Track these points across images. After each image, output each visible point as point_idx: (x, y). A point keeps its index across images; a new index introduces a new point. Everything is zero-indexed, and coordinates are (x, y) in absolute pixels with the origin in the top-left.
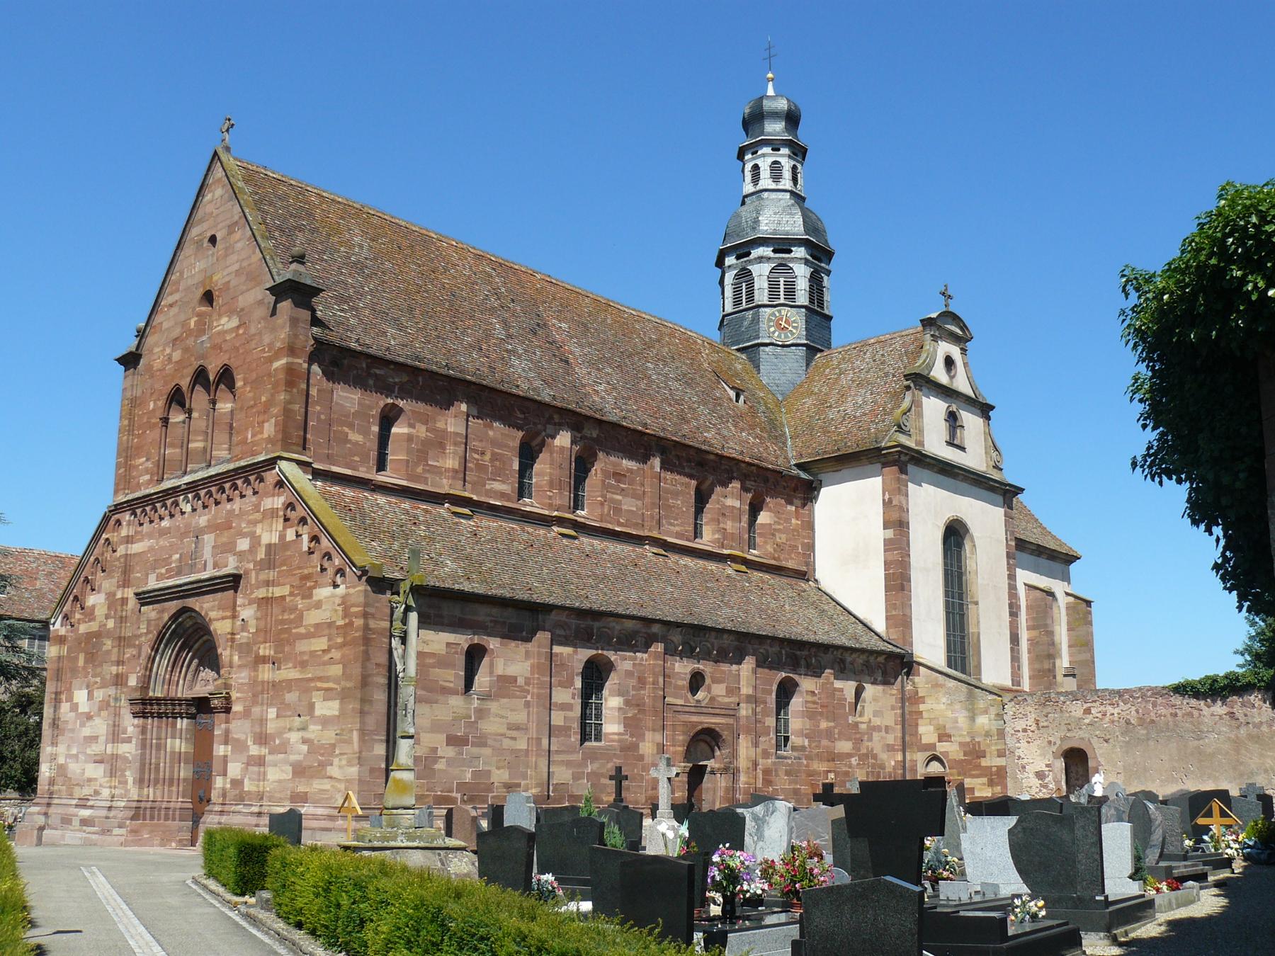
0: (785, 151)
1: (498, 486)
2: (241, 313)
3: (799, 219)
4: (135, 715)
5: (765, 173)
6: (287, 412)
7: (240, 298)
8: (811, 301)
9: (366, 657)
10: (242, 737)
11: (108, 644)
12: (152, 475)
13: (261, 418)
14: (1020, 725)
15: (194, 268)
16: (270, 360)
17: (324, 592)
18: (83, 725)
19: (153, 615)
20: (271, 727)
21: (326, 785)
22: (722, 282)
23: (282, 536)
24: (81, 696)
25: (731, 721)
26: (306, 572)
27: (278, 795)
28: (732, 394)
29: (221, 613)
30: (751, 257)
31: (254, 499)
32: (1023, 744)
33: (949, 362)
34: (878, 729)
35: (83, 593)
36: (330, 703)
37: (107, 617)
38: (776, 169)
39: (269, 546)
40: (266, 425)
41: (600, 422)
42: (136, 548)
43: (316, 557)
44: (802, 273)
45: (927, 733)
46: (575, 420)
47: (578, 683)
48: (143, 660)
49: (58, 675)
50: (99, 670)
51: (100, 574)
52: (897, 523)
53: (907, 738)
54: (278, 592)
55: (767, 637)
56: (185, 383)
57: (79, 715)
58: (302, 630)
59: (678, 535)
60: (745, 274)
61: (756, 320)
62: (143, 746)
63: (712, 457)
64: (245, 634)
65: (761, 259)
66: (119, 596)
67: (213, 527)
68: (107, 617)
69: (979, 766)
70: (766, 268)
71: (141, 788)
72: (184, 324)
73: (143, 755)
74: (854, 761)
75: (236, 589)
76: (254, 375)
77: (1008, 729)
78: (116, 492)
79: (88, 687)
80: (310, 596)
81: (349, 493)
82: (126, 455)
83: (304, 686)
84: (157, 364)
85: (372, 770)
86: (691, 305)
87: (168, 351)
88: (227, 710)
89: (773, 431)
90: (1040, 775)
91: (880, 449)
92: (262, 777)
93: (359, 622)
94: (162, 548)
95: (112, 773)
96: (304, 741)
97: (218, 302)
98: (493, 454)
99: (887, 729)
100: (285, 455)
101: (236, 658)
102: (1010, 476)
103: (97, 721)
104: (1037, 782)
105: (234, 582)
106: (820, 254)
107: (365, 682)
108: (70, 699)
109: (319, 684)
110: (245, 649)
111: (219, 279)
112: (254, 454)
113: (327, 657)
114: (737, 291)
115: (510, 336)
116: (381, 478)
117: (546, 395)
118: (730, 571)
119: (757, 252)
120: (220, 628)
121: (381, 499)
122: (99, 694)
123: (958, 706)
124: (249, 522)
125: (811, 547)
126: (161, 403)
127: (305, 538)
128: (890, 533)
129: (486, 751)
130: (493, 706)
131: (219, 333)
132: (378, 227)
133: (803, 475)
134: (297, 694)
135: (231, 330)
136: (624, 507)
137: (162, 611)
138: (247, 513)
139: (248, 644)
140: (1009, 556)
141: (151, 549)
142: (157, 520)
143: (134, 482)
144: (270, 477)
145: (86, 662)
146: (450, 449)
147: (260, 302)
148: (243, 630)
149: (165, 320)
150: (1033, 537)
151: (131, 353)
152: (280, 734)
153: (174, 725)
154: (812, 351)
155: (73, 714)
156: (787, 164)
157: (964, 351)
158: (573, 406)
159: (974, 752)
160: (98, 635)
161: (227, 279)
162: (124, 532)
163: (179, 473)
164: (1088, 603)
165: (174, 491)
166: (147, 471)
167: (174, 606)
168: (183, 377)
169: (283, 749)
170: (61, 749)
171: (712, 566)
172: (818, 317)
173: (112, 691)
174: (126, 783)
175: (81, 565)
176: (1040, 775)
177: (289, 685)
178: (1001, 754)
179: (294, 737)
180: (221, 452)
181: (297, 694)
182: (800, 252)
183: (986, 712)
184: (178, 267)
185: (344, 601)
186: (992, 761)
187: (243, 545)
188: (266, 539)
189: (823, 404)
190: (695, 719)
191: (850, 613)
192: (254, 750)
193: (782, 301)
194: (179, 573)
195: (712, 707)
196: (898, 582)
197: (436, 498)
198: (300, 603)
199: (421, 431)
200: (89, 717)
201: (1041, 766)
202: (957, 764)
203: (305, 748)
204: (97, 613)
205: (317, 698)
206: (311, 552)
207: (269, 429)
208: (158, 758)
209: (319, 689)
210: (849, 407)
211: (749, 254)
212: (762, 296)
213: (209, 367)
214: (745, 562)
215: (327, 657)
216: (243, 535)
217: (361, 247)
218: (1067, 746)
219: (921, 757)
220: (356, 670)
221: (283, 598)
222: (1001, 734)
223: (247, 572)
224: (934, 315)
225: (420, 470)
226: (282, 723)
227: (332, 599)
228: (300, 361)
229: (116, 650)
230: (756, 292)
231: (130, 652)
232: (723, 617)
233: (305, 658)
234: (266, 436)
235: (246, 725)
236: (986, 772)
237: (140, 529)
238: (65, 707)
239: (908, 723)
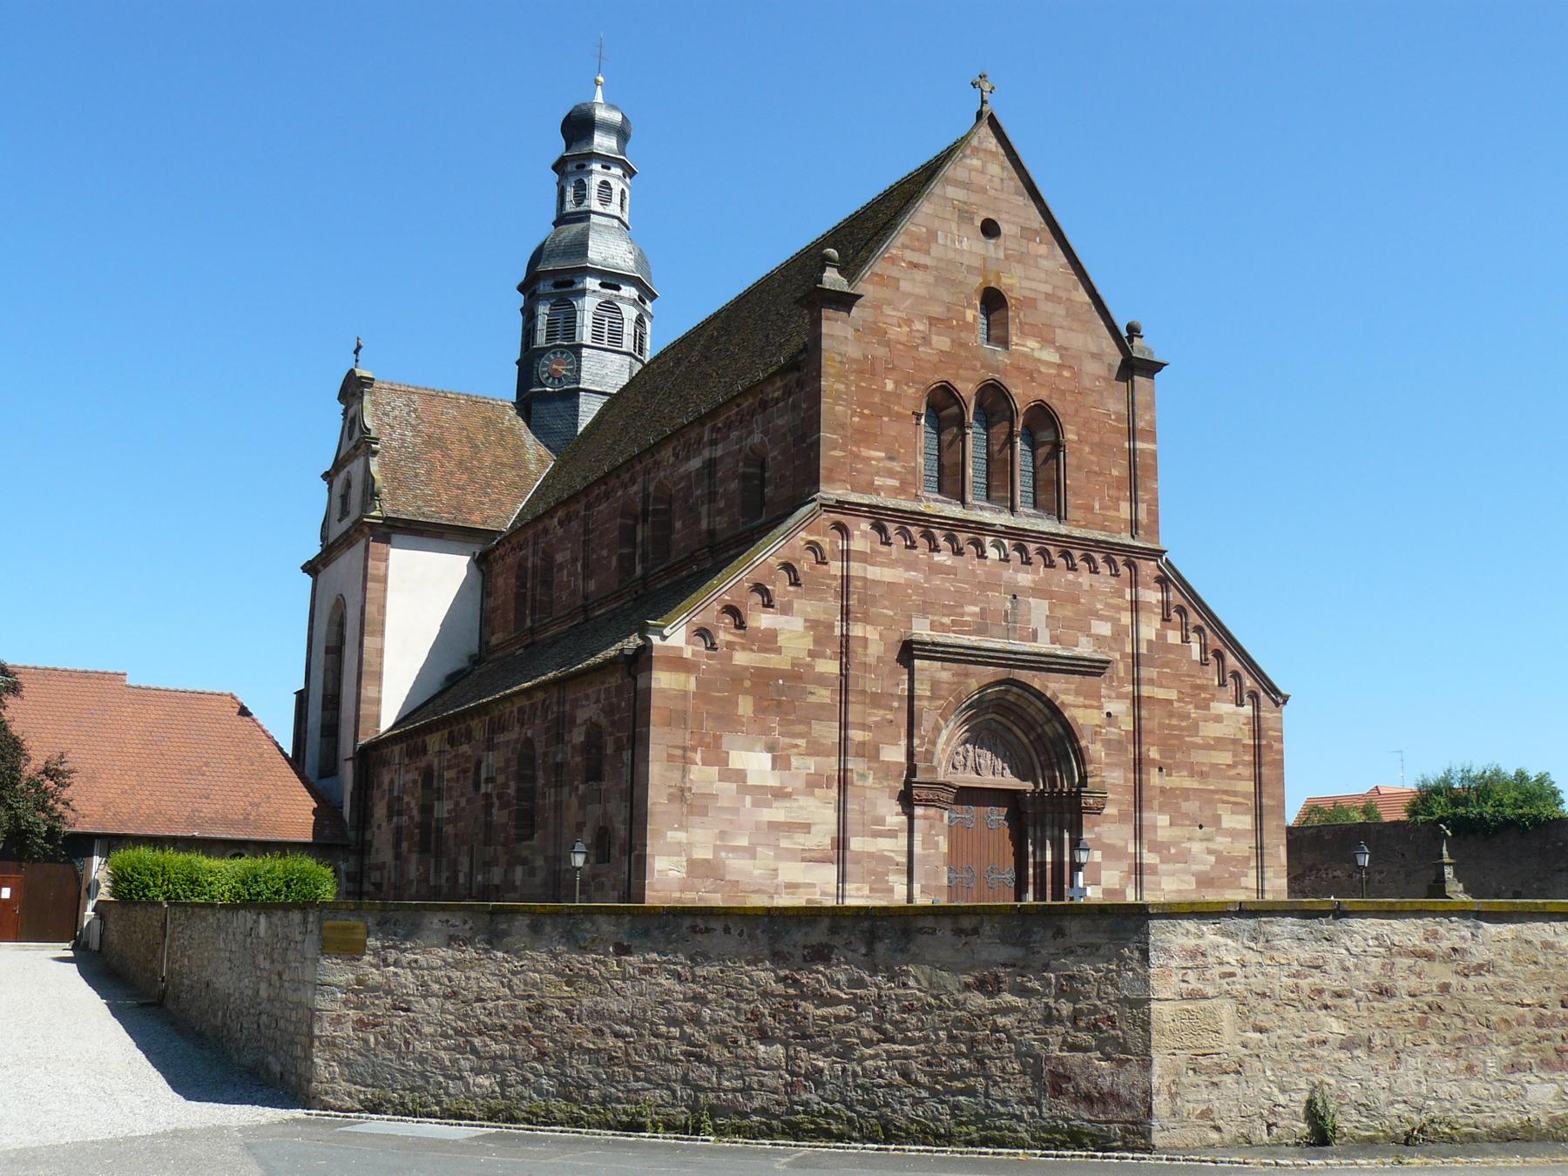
23: (1161, 636)
29: (1081, 700)
31: (1113, 581)
36: (1241, 818)
42: (874, 573)
58: (1198, 740)
76: (1096, 438)
80: (1207, 708)
87: (919, 326)
96: (1210, 852)
105: (1093, 669)
109: (1225, 798)
124: (1107, 605)
131: (1024, 354)
134: (1197, 804)
135: (1049, 364)
137: (967, 675)
139: (1119, 742)
141: (909, 584)
147: (1094, 356)
152: (1175, 844)
165: (983, 527)
166: (891, 474)
167: (990, 673)
168: (957, 376)
169: (1184, 857)
177: (1186, 794)
179: (1196, 847)
181: (1197, 804)
187: (1104, 629)
194: (981, 630)
203: (1213, 859)
204: (781, 640)
206: (1204, 663)
209: (1224, 802)
215: (1233, 772)
221: (1170, 702)
226: (1177, 832)
237: (885, 549)
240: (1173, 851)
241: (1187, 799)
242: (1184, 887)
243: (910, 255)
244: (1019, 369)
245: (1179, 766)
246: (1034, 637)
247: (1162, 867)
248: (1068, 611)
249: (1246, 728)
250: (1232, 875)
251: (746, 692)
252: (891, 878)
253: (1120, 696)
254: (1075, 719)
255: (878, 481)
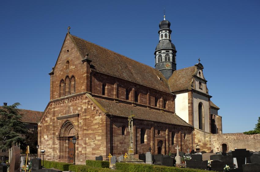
0: (168, 31)
1: (122, 97)
2: (75, 65)
3: (171, 45)
4: (58, 140)
5: (164, 36)
6: (87, 84)
7: (75, 62)
8: (173, 61)
9: (106, 129)
10: (81, 143)
11: (51, 127)
12: (58, 96)
13: (81, 85)
14: (214, 139)
15: (64, 56)
16: (83, 74)
17: (97, 117)
18: (46, 142)
19: (61, 122)
20: (87, 142)
21: (99, 152)
22: (155, 57)
23: (88, 107)
24: (46, 137)
25: (165, 139)
26: (93, 113)
27: (89, 153)
28: (159, 79)
29: (75, 121)
30: (162, 52)
32: (215, 143)
33: (200, 73)
34: (188, 140)
35: (45, 118)
37: (50, 122)
38: (166, 35)
39: (85, 109)
40: (83, 86)
41: (139, 85)
42: (56, 109)
43: (95, 111)
44: (171, 55)
45: (196, 141)
46: (135, 85)
47: (140, 133)
48: (59, 130)
49: (41, 133)
50: (49, 132)
51: (48, 114)
52: (191, 103)
53: (193, 142)
54: (87, 117)
55: (170, 124)
56: (64, 79)
57: (46, 140)
58: (93, 124)
59: (153, 106)
60: (160, 56)
61: (163, 65)
62: (60, 146)
63: (158, 91)
64: (81, 125)
65: (164, 53)
66: (53, 118)
67: (72, 105)
68: (50, 122)
69: (206, 147)
70: (165, 55)
71: (60, 153)
72: (63, 67)
73: (60, 147)
74: (184, 146)
75: (78, 116)
76: (79, 77)
77: (212, 140)
78: (51, 99)
79: (47, 135)
80: (94, 118)
81: (98, 99)
82: (52, 92)
83: (94, 134)
84: (58, 75)
85: (108, 149)
86: (150, 62)
87: (60, 72)
88: (78, 139)
89: (167, 86)
90: (218, 148)
91: (188, 89)
92: (86, 150)
93: (105, 123)
94: (62, 109)
95: (54, 151)
96: (94, 144)
97: (70, 63)
98: (122, 91)
99: (189, 140)
100: (87, 92)
101: (79, 129)
102: (210, 94)
103: (50, 141)
104: (217, 150)
105: (78, 115)
106: (174, 52)
107: (106, 133)
108: (43, 137)
109: (97, 134)
110: (81, 128)
111: (70, 59)
112: (80, 92)
113: (98, 129)
114: (159, 59)
115: (122, 69)
116: (103, 96)
117: (130, 80)
118: (161, 112)
119: (163, 51)
120: (76, 124)
121: (104, 100)
122: (50, 136)
123: (202, 136)
124: (80, 105)
125: (174, 107)
126: (59, 82)
127: (93, 107)
128: (189, 105)
129: (126, 145)
130: (127, 137)
131: (71, 69)
132: (98, 48)
133: (174, 94)
135: (74, 69)
136: (143, 101)
137: (63, 121)
138: (80, 103)
139: (81, 127)
140: (209, 109)
141: (59, 110)
142: (60, 104)
143: (54, 97)
144: (84, 96)
145: (46, 130)
146: (114, 90)
147: (80, 63)
148: (80, 124)
149: (59, 66)
150: (212, 105)
151: (52, 73)
152: (89, 143)
153: (66, 141)
154: (173, 71)
155: (44, 140)
156: (168, 34)
157: (202, 71)
158: (135, 82)
159: (205, 144)
160: (49, 125)
161: (72, 59)
162: (53, 107)
163: (64, 95)
164: (221, 117)
165: (64, 99)
166: (57, 95)
167: (65, 120)
168: (63, 77)
169: (90, 145)
170: (42, 146)
171: (158, 111)
172: (174, 64)
173: (53, 136)
174: (57, 152)
175: (44, 113)
176: (218, 148)
177: (91, 134)
178: (210, 145)
179: (92, 143)
180: (73, 92)
182: (171, 51)
183: (207, 137)
184: (60, 56)
185: (101, 119)
186: (208, 146)
187: (79, 109)
188: (84, 108)
189: (176, 81)
190: (159, 139)
191: (182, 119)
192: (84, 146)
193: (167, 61)
194: (66, 114)
195: (162, 136)
196: (191, 114)
197: (112, 100)
198: (92, 119)
199: (110, 87)
200: (48, 140)
201: (218, 147)
202: (201, 146)
203: (95, 145)
204: (48, 121)
205: (97, 136)
206: (94, 110)
207: (83, 87)
208: (63, 148)
209: (97, 135)
210: (181, 81)
211: (161, 52)
212: (163, 60)
213: (69, 75)
214: (163, 110)
215: (98, 129)
216: (79, 107)
217: (95, 52)
218: (223, 143)
219: (195, 145)
220: (105, 131)
221: (88, 118)
222: (210, 141)
223: (80, 114)
224: (197, 64)
225: (110, 94)
226: (89, 141)
227: (99, 119)
228: (89, 74)
229: (53, 128)
230: (163, 60)
231: (56, 129)
232: (162, 120)
233: (94, 129)
234: (83, 88)
235: (82, 141)
236: (207, 148)
237: (56, 106)
238: (42, 139)
239: (193, 139)
240: (89, 144)
241: (91, 135)
242: (90, 150)
243: (59, 62)
244: (70, 72)
245: (90, 129)
246: (71, 113)
247: (87, 147)
248: (75, 107)
249: (100, 120)
250: (98, 148)
251: (45, 128)
252: (57, 150)
253: (81, 119)
254: (74, 124)
255: (56, 97)
